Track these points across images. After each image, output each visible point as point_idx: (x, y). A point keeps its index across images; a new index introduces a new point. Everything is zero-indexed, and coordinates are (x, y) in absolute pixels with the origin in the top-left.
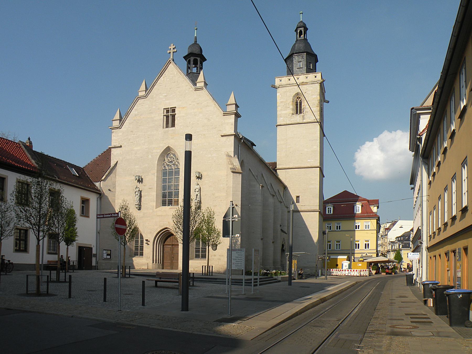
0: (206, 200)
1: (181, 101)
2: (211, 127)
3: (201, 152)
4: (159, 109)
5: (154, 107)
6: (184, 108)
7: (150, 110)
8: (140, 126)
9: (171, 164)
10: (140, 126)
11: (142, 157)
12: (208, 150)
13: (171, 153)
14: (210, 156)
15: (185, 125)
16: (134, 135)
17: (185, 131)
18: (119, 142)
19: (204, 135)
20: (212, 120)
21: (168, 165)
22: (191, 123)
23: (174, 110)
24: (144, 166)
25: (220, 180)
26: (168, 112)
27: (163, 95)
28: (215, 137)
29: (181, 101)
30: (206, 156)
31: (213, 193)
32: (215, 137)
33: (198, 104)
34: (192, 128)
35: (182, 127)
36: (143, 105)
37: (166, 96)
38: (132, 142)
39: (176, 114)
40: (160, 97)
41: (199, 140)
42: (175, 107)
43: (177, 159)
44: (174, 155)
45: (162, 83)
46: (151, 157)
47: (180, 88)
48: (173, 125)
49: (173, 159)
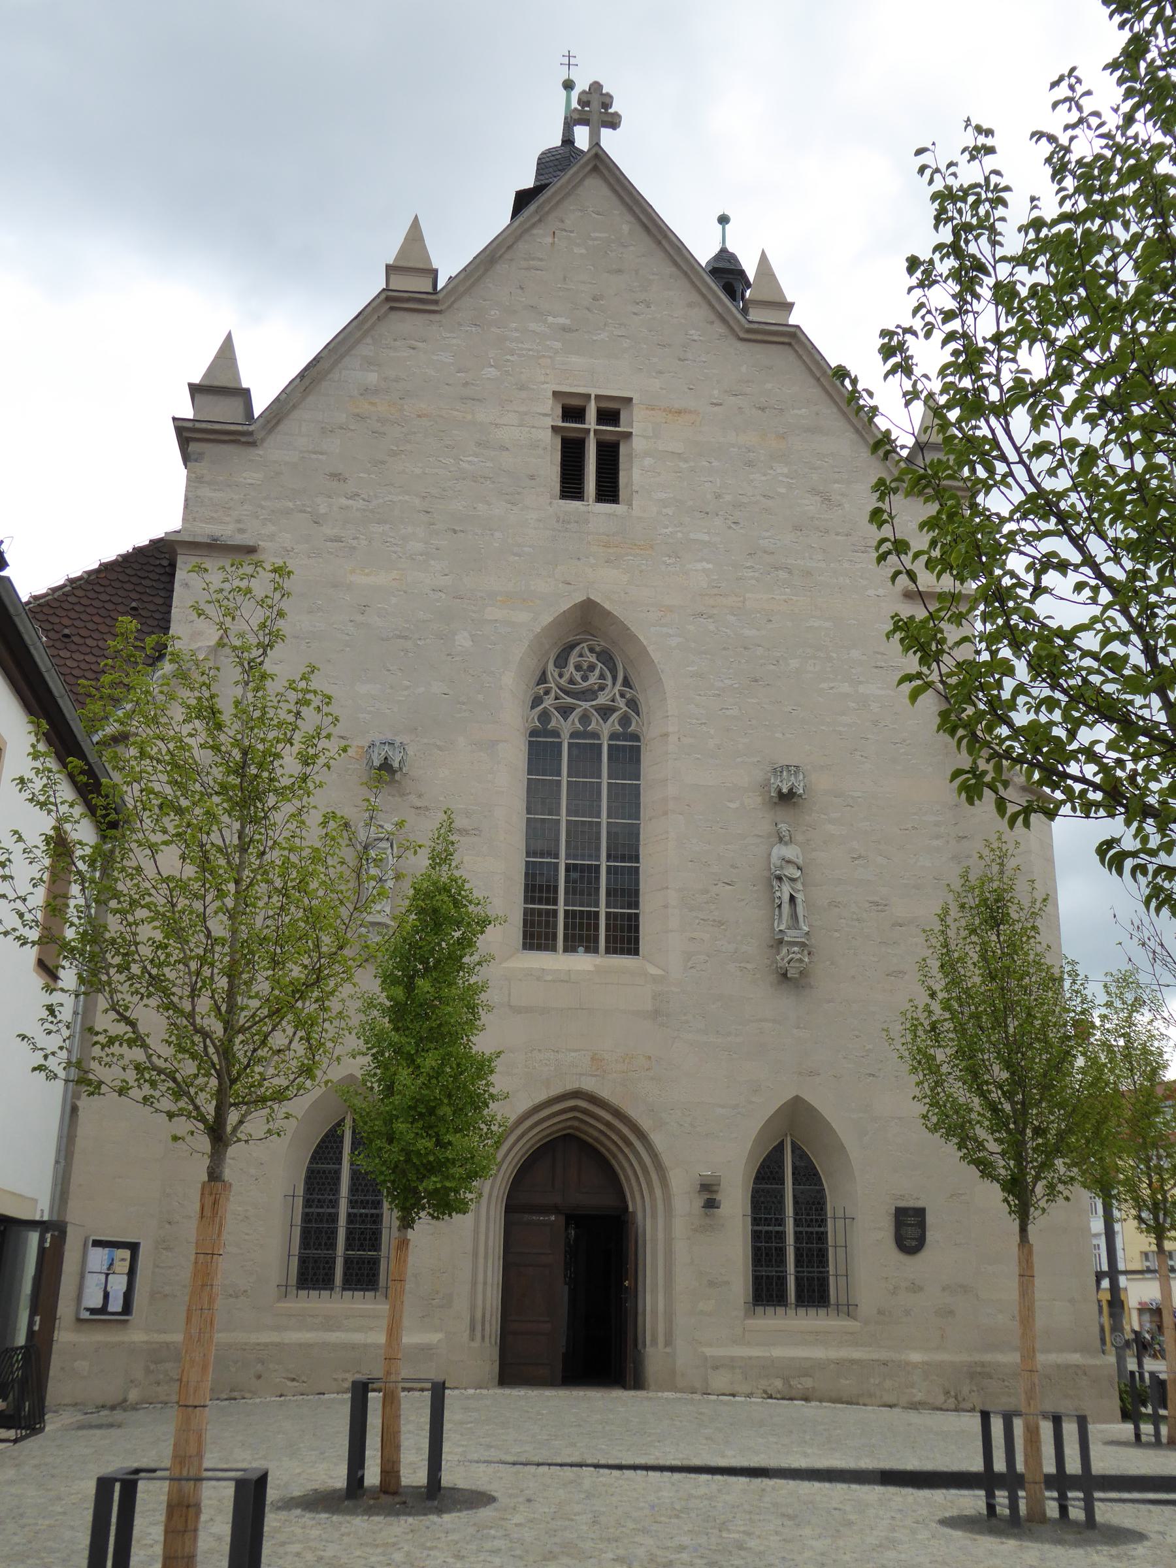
0: (837, 934)
1: (661, 372)
2: (839, 538)
3: (794, 663)
4: (522, 388)
5: (492, 372)
6: (679, 412)
7: (466, 384)
8: (393, 454)
9: (586, 705)
10: (393, 454)
11: (405, 638)
12: (834, 655)
13: (584, 645)
14: (845, 688)
15: (690, 503)
16: (351, 502)
17: (692, 536)
18: (239, 521)
19: (808, 573)
20: (847, 506)
21: (565, 711)
22: (728, 498)
23: (609, 416)
24: (422, 689)
25: (914, 828)
26: (573, 413)
27: (550, 319)
28: (871, 592)
29: (661, 372)
30: (824, 685)
31: (876, 899)
32: (871, 592)
33: (763, 409)
34: (730, 528)
35: (670, 511)
36: (420, 345)
37: (565, 329)
38: (338, 539)
39: (628, 435)
40: (533, 326)
41: (778, 597)
42: (629, 400)
43: (627, 683)
44: (606, 657)
45: (541, 260)
46: (468, 644)
47: (653, 308)
48: (609, 491)
49: (602, 676)
